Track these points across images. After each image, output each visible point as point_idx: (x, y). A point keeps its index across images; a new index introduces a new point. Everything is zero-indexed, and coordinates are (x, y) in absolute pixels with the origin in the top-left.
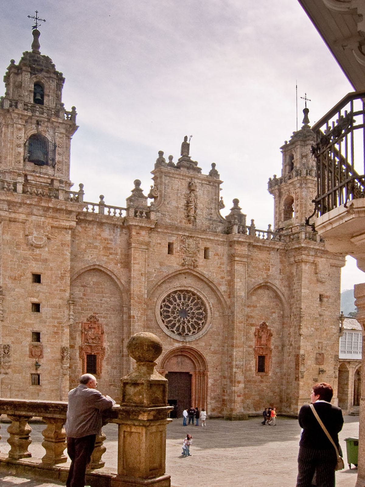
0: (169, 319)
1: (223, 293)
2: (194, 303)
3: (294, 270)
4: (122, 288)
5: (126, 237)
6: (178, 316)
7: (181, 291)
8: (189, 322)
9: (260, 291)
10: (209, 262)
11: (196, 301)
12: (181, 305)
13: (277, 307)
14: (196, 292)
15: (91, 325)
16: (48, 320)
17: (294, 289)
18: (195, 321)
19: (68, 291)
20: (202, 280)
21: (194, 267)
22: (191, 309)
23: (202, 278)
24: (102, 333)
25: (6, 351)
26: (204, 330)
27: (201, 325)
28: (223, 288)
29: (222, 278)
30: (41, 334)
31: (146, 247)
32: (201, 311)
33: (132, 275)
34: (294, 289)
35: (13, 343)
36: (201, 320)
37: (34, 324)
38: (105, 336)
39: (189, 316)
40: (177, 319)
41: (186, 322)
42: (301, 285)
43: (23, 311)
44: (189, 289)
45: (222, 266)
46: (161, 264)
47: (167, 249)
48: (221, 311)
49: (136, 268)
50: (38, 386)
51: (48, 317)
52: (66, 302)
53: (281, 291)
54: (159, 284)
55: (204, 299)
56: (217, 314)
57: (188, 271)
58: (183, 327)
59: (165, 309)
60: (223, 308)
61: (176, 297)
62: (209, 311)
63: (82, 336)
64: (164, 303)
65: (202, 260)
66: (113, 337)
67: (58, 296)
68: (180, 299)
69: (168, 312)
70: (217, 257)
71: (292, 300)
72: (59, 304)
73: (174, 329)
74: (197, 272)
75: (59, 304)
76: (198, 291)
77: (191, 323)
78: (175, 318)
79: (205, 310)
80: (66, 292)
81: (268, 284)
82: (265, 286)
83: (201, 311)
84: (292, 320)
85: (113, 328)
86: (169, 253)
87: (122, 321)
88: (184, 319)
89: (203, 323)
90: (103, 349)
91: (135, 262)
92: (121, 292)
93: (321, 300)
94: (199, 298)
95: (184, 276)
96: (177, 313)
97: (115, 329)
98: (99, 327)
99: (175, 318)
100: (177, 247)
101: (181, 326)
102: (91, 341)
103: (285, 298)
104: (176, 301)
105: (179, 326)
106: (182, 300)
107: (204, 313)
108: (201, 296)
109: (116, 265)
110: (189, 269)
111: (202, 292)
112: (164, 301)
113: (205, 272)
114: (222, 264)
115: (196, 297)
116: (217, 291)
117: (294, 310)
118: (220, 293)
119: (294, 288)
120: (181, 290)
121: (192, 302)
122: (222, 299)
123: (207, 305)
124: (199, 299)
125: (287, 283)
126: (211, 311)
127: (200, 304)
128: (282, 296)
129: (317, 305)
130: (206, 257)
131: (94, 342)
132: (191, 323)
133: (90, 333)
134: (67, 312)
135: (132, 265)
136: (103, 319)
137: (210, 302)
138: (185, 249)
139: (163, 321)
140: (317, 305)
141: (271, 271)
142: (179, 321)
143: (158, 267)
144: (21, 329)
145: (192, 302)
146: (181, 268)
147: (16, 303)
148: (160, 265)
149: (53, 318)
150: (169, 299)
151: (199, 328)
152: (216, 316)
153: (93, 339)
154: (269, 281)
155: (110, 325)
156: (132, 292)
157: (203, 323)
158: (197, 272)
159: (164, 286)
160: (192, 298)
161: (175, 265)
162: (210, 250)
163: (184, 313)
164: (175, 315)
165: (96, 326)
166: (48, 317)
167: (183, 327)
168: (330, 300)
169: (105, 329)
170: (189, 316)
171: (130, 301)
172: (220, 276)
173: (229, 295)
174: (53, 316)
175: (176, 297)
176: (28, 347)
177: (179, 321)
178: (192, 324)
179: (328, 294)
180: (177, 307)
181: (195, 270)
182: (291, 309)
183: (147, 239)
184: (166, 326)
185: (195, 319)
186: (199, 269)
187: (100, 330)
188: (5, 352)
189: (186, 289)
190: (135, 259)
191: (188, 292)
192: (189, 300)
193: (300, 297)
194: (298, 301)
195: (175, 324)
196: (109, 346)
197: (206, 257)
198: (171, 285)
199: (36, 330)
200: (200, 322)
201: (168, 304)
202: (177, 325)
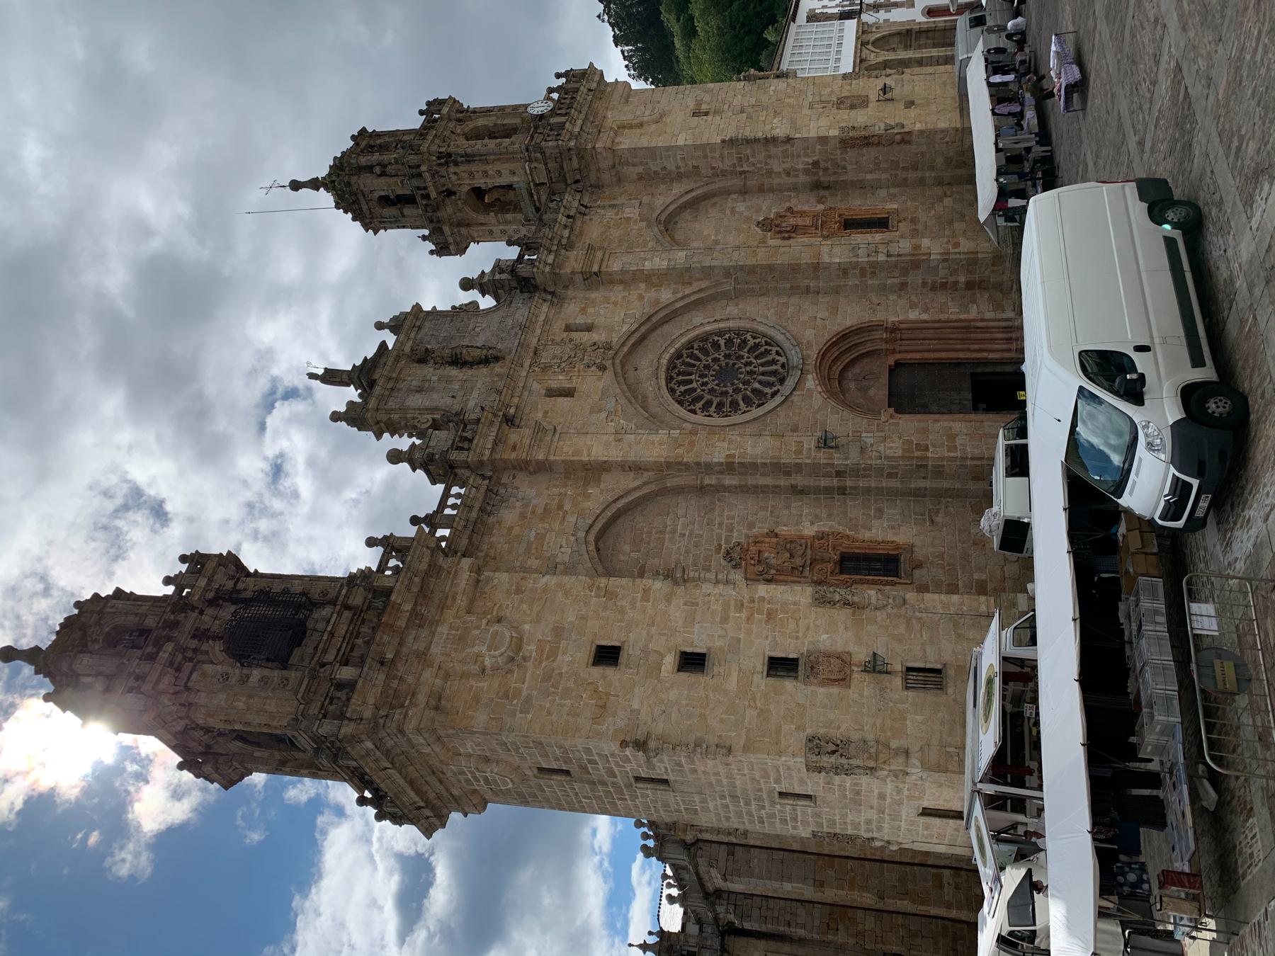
0: (741, 403)
1: (680, 295)
2: (701, 356)
3: (633, 171)
4: (653, 487)
5: (521, 476)
6: (733, 384)
7: (669, 379)
8: (749, 364)
9: (680, 236)
10: (600, 321)
11: (696, 352)
12: (705, 380)
13: (721, 206)
14: (672, 350)
15: (752, 558)
16: (731, 634)
17: (678, 167)
18: (748, 352)
19: (647, 582)
20: (643, 338)
21: (610, 349)
22: (715, 360)
23: (637, 335)
24: (776, 535)
25: (831, 747)
26: (772, 332)
27: (757, 341)
28: (666, 295)
29: (641, 297)
30: (773, 654)
31: (550, 433)
32: (722, 342)
33: (619, 459)
34: (678, 167)
35: (800, 728)
36: (745, 341)
37: (740, 669)
38: (784, 530)
39: (734, 364)
40: (741, 386)
41: (748, 368)
42: (669, 148)
43: (702, 694)
44: (664, 362)
45: (613, 299)
46: (596, 410)
47: (561, 400)
48: (724, 302)
49: (597, 448)
50: (943, 672)
51: (721, 632)
52: (680, 590)
53: (681, 196)
54: (647, 415)
55: (693, 334)
56: (732, 310)
57: (618, 361)
58: (763, 374)
59: (713, 409)
60: (714, 298)
61: (682, 388)
62: (721, 325)
63: (783, 581)
64: (699, 411)
65: (594, 335)
66: (786, 512)
67: (662, 606)
68: (691, 382)
69: (720, 405)
70: (591, 310)
71: (703, 172)
72: (685, 604)
73: (768, 391)
74: (623, 345)
75: (685, 604)
76: (670, 345)
77: (752, 359)
78: (737, 390)
79: (721, 333)
80: (650, 589)
81: (663, 218)
82: (667, 224)
83: (722, 342)
84: (751, 169)
85: (761, 513)
86: (573, 396)
87: (744, 489)
88: (741, 373)
89: (754, 338)
90: (821, 536)
91: (585, 454)
92: (664, 492)
93: (707, 114)
94: (689, 345)
95: (631, 373)
96: (724, 386)
97: (764, 508)
98: (756, 542)
99: (737, 390)
100: (559, 380)
101: (760, 377)
102: (798, 561)
103: (699, 187)
104: (694, 390)
105: (760, 382)
106: (693, 377)
107: (727, 336)
108: (684, 340)
109: (589, 497)
110: (613, 358)
111: (674, 337)
112: (694, 412)
113: (624, 330)
114: (607, 300)
115: (684, 352)
116: (673, 308)
117: (726, 165)
118: (676, 301)
119: (673, 168)
120: (666, 379)
121: (699, 360)
122: (692, 298)
123: (708, 328)
124: (692, 348)
125: (662, 186)
126: (722, 320)
127: (706, 342)
128: (694, 194)
129: (718, 118)
130: (589, 328)
131: (800, 553)
132: (752, 359)
133: (773, 561)
134: (707, 588)
135: (592, 459)
136: (735, 534)
137: (701, 323)
138: (563, 365)
139: (745, 412)
140: (718, 118)
141: (632, 215)
142: (746, 383)
143: (604, 415)
144: (758, 702)
145: (699, 360)
146: (609, 374)
147: (675, 708)
148: (600, 411)
149: (725, 619)
150: (687, 400)
151: (767, 343)
152: (736, 311)
153: (792, 556)
154: (655, 216)
155: (751, 518)
156: (663, 460)
157: (754, 338)
158: (623, 345)
159: (654, 408)
160: (688, 360)
161: (601, 384)
162: (571, 321)
163: (725, 374)
164: (731, 391)
165: (753, 549)
166: (721, 632)
167: (763, 374)
168: (707, 98)
169: (761, 529)
170: (734, 364)
171: (687, 466)
172: (636, 302)
173: (683, 284)
174: (718, 620)
175: (682, 388)
176: (813, 688)
177: (746, 383)
178: (756, 358)
179: (692, 105)
180: (709, 387)
181: (615, 345)
182: (724, 173)
183: (527, 432)
184: (759, 406)
185: (744, 353)
186: (615, 339)
187: (767, 540)
188: (834, 752)
189: (664, 369)
190: (576, 453)
191: (672, 366)
192: (694, 366)
193: (695, 147)
194: (705, 156)
195: (754, 391)
196: (812, 523)
197: (589, 328)
198: (651, 396)
199: (761, 666)
200: (751, 342)
201: (700, 405)
202: (756, 385)
